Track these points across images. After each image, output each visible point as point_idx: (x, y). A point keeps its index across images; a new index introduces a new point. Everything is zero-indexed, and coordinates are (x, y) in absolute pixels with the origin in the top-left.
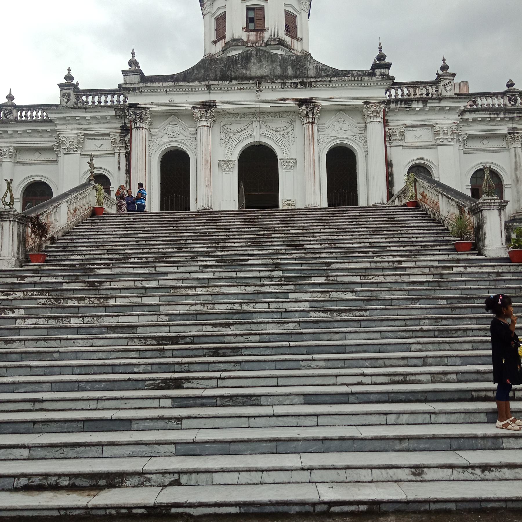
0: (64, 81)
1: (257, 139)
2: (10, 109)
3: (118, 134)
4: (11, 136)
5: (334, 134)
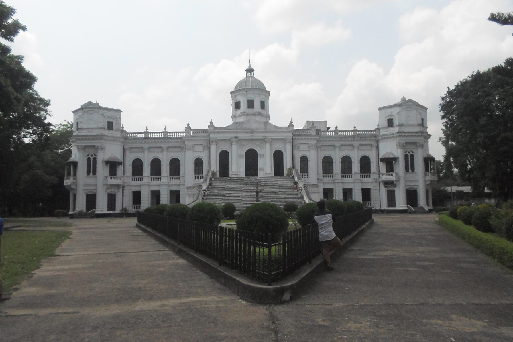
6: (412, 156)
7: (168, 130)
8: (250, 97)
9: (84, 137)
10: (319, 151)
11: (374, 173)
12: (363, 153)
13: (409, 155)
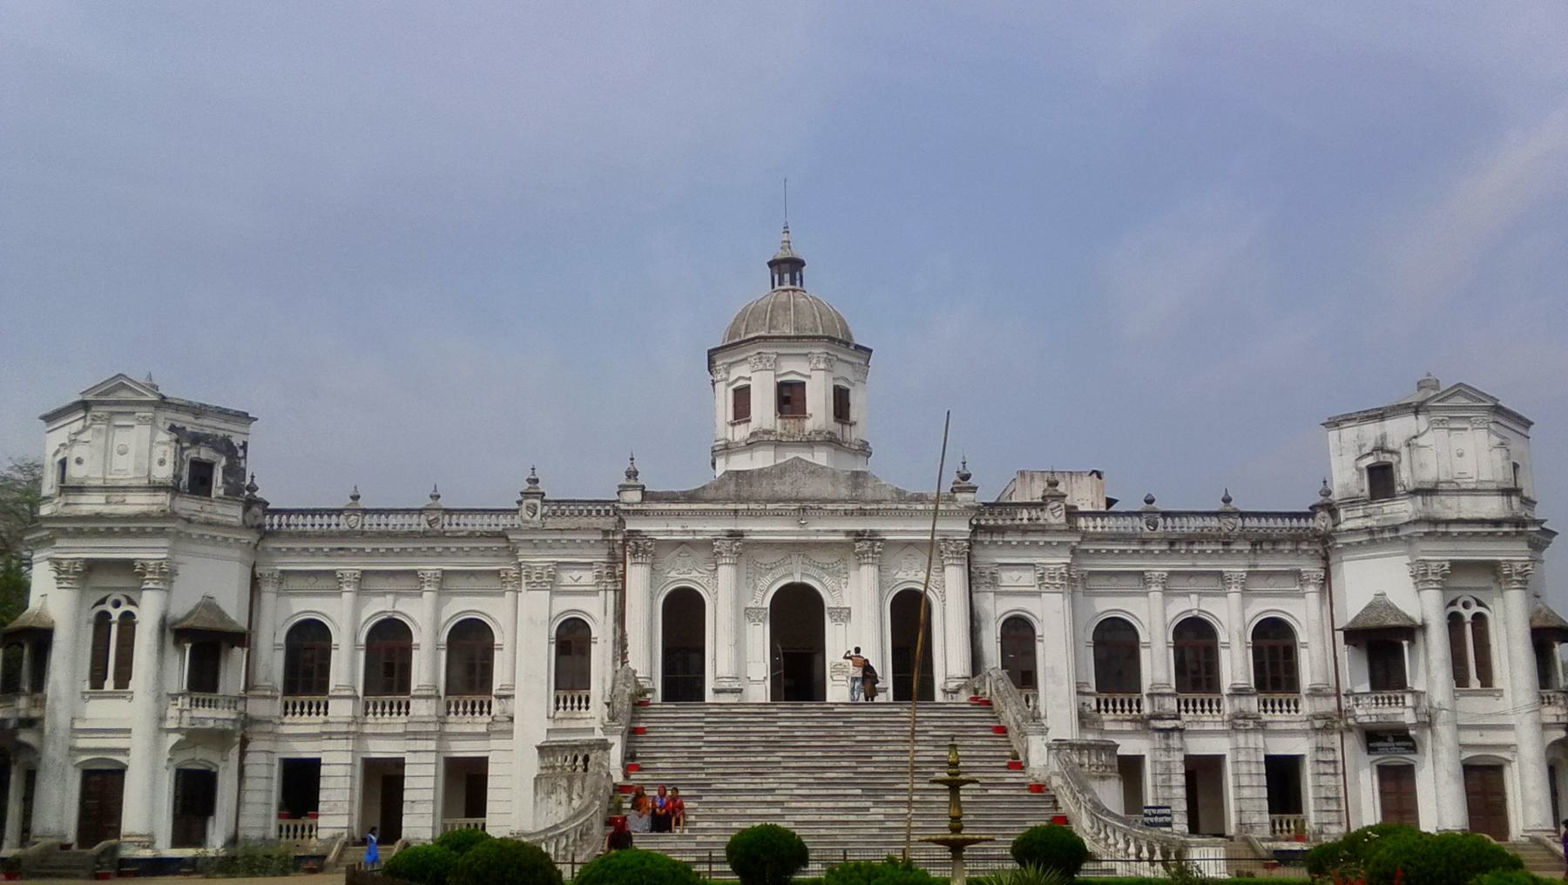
0: (526, 486)
1: (797, 579)
2: (439, 515)
4: (440, 554)
5: (901, 575)
6: (1479, 620)
7: (444, 503)
8: (793, 368)
9: (87, 526)
10: (1080, 595)
11: (1315, 693)
12: (1262, 607)
13: (1467, 615)
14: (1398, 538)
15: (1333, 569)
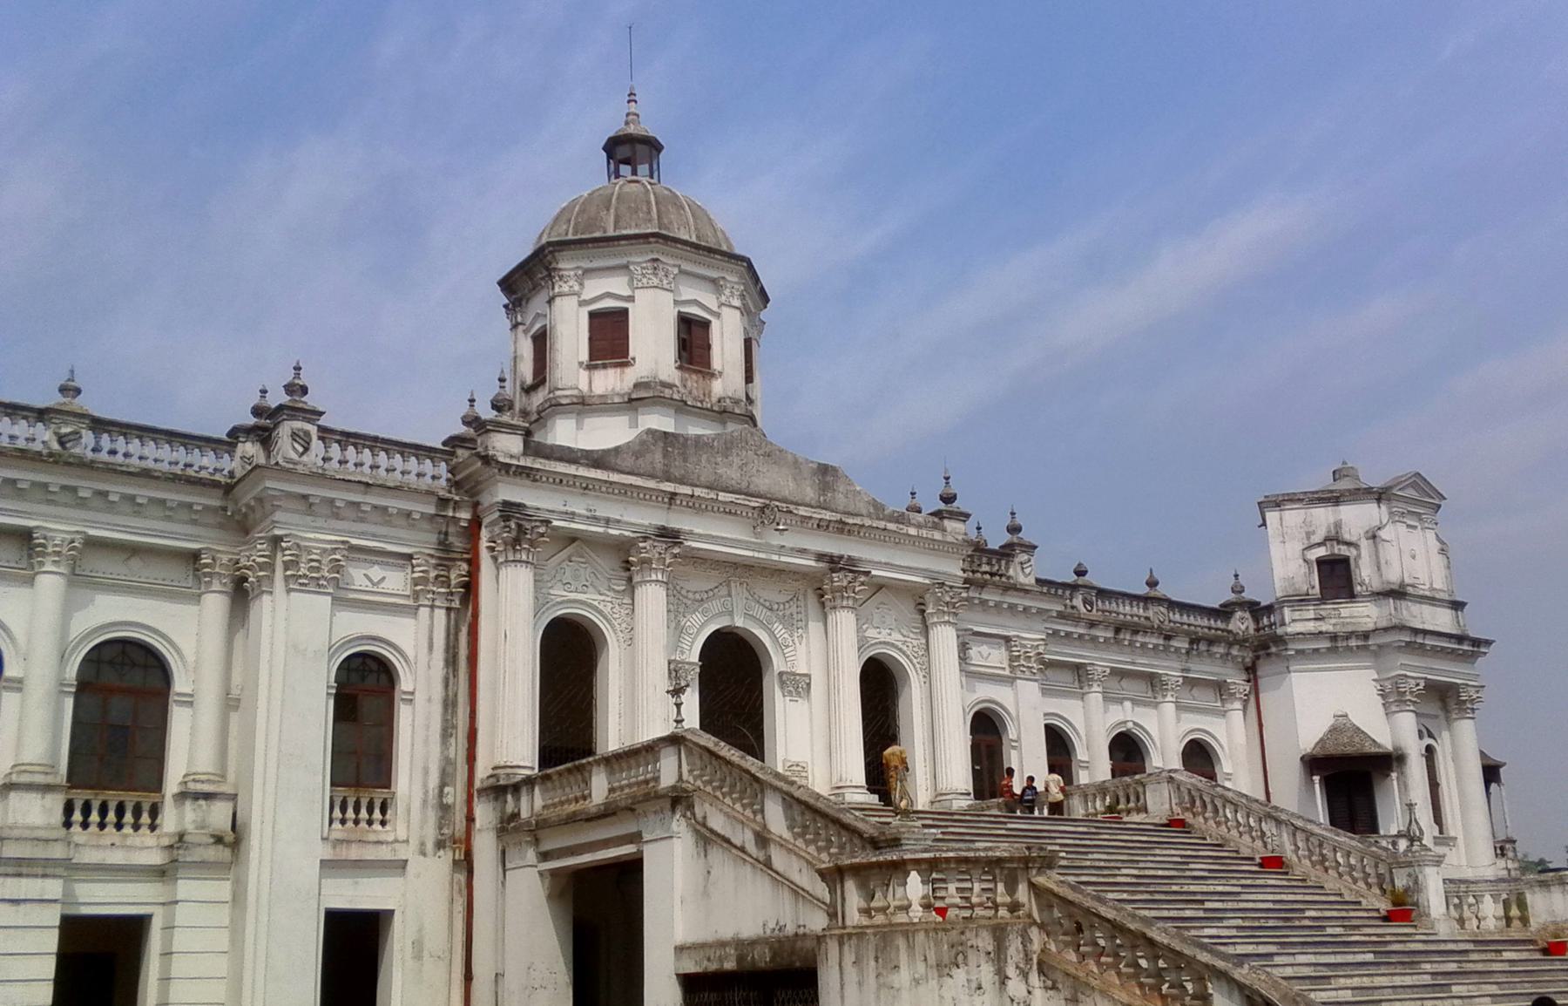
1: (739, 622)
3: (433, 561)
4: (82, 504)
14: (1366, 647)
15: (1260, 682)
